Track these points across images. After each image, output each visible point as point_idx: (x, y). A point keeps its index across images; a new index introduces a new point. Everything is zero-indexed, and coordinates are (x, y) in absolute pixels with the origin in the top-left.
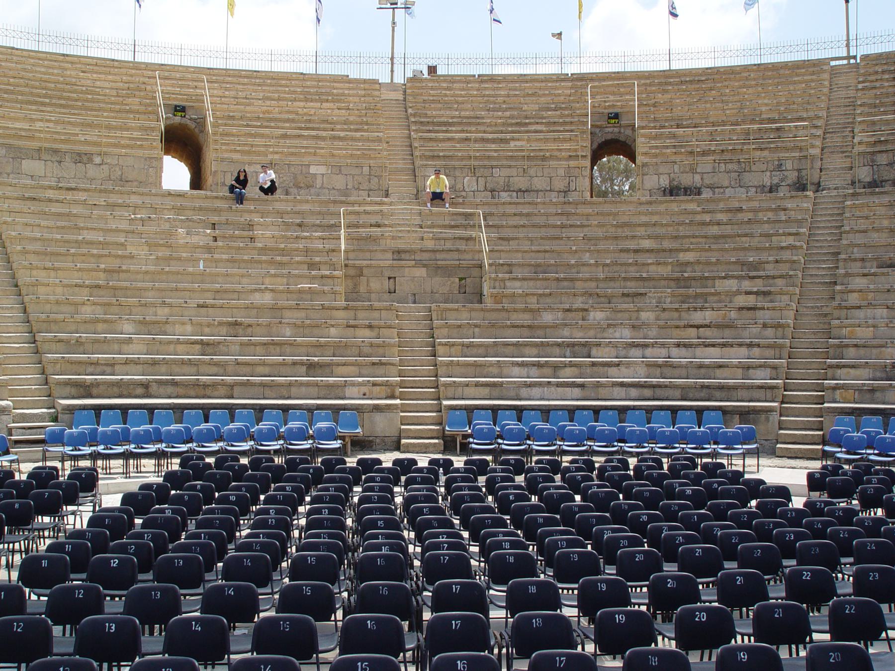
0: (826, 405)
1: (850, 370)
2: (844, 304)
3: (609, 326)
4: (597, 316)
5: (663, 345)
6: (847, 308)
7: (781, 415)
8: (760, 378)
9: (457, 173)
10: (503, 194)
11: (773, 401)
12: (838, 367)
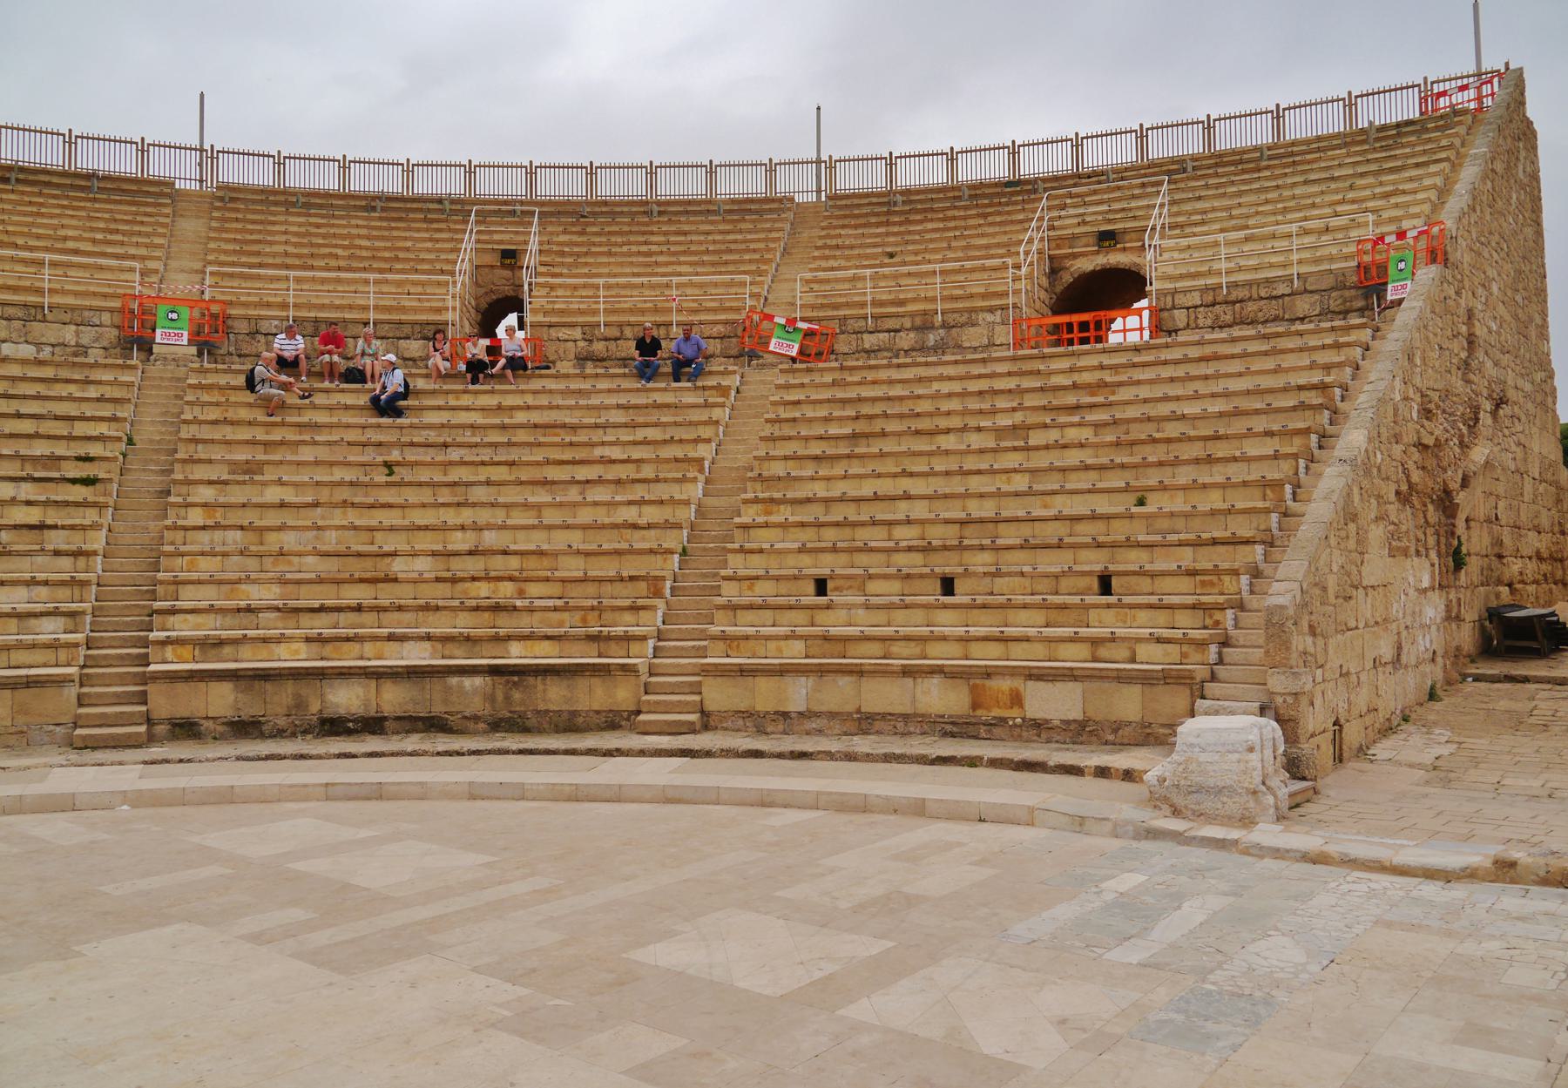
0: (152, 668)
1: (188, 616)
2: (180, 523)
6: (185, 529)
7: (81, 685)
8: (49, 629)
11: (69, 665)
12: (173, 611)
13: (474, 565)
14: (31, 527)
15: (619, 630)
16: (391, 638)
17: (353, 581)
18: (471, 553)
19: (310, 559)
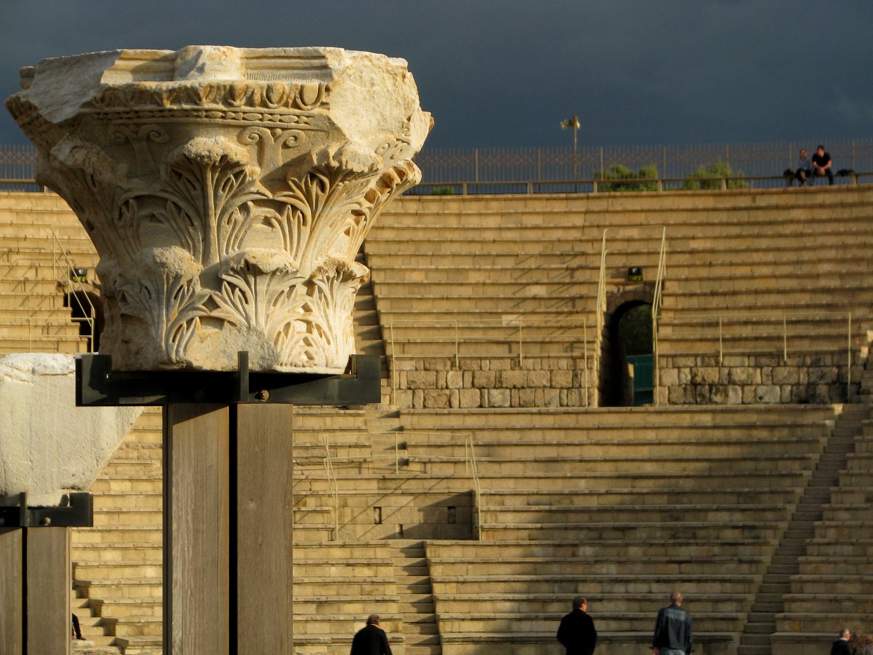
3: (596, 562)
4: (587, 551)
5: (644, 581)
9: (440, 367)
10: (494, 392)
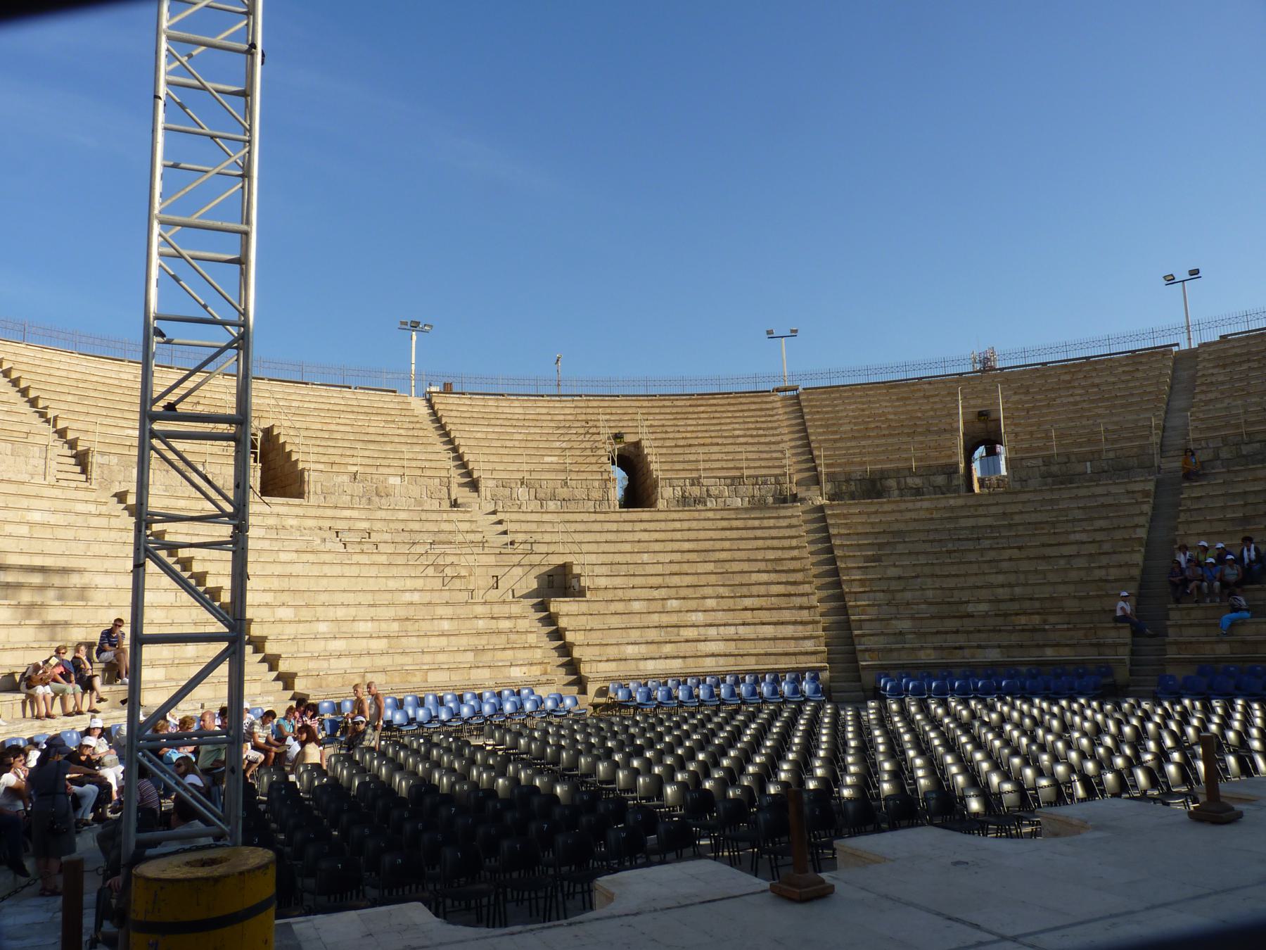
10: (550, 503)
13: (1015, 606)
14: (784, 595)
15: (1110, 641)
16: (979, 647)
17: (950, 617)
18: (1011, 600)
19: (923, 606)
